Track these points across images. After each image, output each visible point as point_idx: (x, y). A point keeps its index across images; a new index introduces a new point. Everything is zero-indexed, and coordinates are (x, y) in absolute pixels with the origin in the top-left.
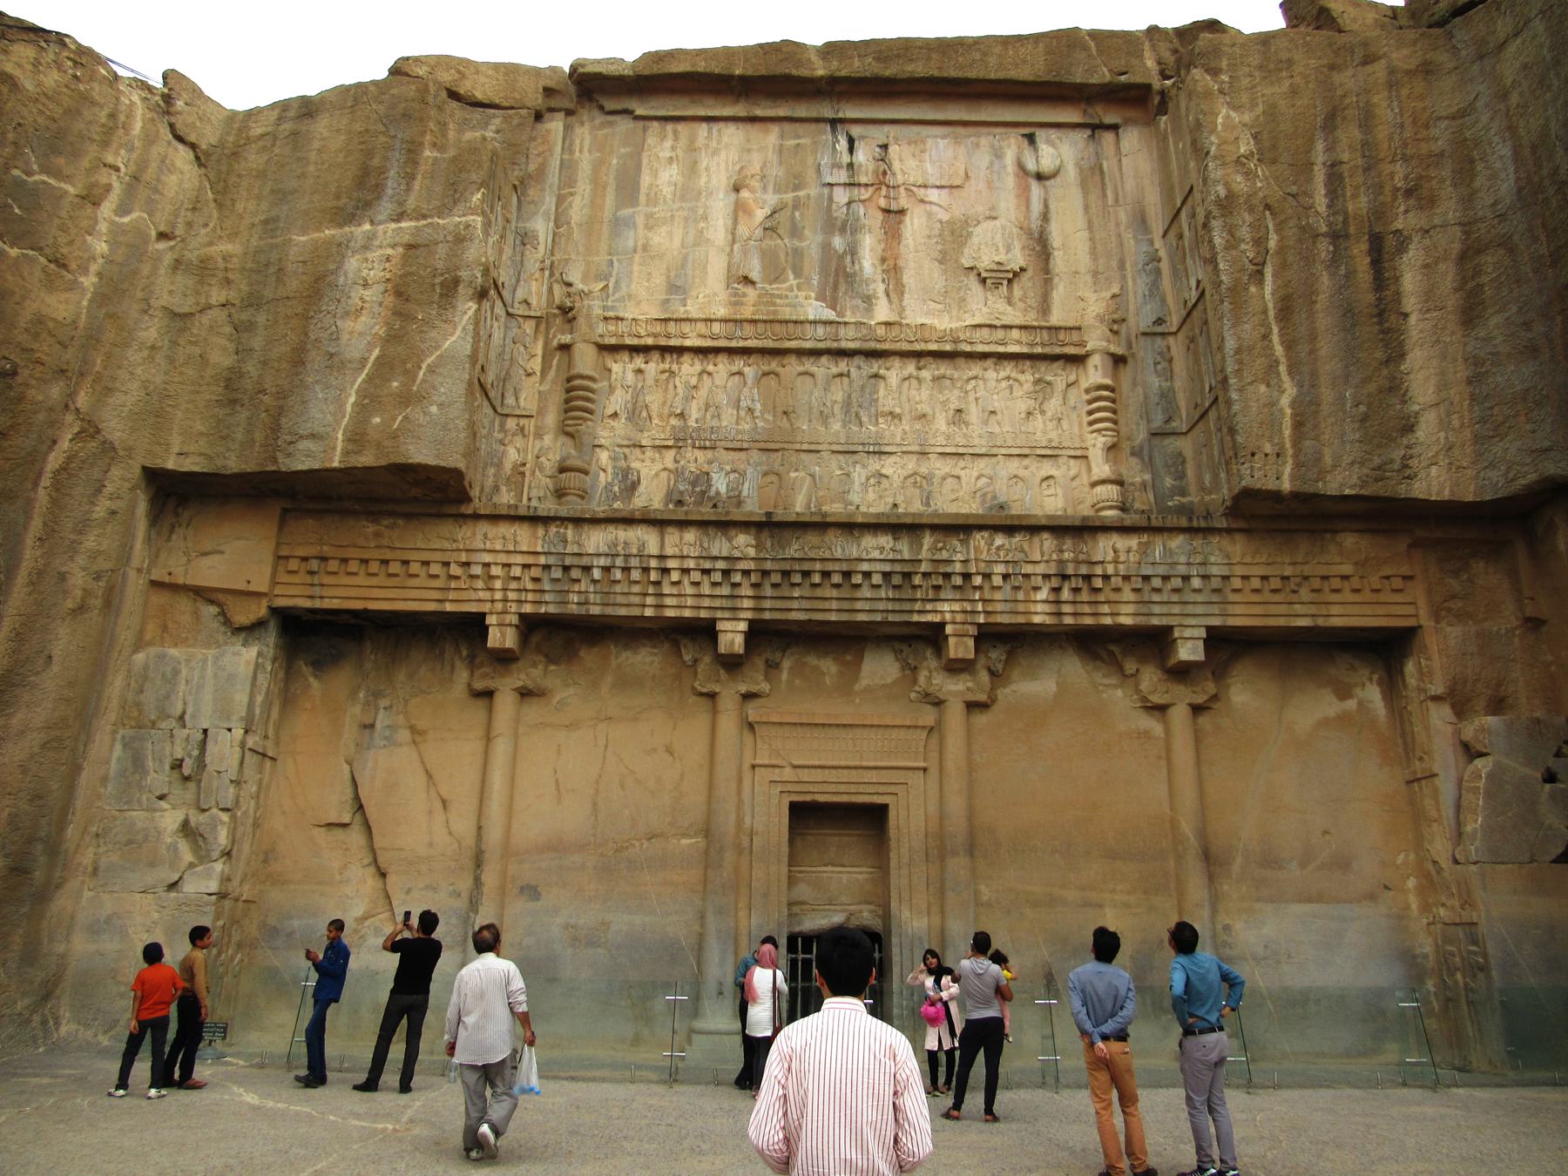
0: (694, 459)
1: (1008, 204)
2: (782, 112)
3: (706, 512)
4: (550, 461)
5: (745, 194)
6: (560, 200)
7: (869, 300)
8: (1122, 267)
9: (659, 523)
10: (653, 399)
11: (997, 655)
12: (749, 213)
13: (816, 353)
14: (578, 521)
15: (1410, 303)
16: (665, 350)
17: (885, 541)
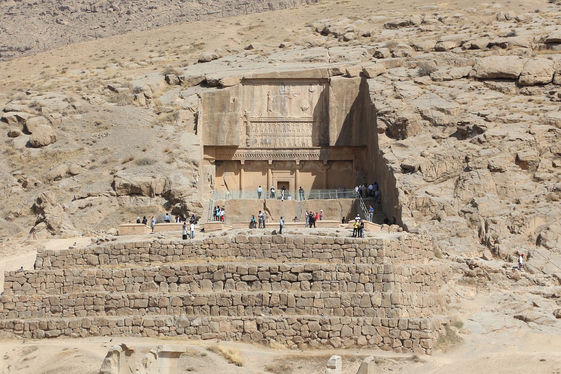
0: (264, 137)
1: (307, 96)
2: (274, 82)
3: (267, 147)
4: (245, 138)
5: (269, 96)
6: (243, 97)
7: (287, 113)
8: (323, 106)
9: (261, 149)
10: (258, 129)
11: (303, 163)
12: (270, 100)
13: (280, 122)
14: (251, 149)
15: (354, 120)
16: (259, 122)
17: (289, 150)
